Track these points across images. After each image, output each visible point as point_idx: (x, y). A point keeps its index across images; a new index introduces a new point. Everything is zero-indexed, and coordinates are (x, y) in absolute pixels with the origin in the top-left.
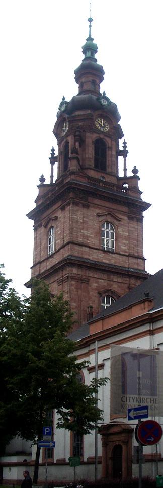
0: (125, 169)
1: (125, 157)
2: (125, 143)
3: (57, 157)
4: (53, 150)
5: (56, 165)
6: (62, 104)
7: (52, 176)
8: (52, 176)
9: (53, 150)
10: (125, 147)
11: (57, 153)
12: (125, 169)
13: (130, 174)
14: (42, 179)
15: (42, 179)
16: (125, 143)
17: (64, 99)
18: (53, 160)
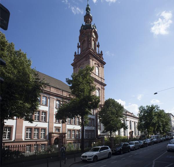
0: (99, 51)
1: (99, 47)
2: (98, 43)
3: (80, 46)
4: (78, 44)
5: (80, 49)
6: (82, 27)
7: (78, 52)
8: (78, 52)
9: (78, 44)
10: (99, 44)
11: (79, 45)
12: (99, 51)
13: (100, 53)
14: (75, 53)
15: (75, 53)
16: (98, 43)
17: (82, 24)
18: (78, 47)
